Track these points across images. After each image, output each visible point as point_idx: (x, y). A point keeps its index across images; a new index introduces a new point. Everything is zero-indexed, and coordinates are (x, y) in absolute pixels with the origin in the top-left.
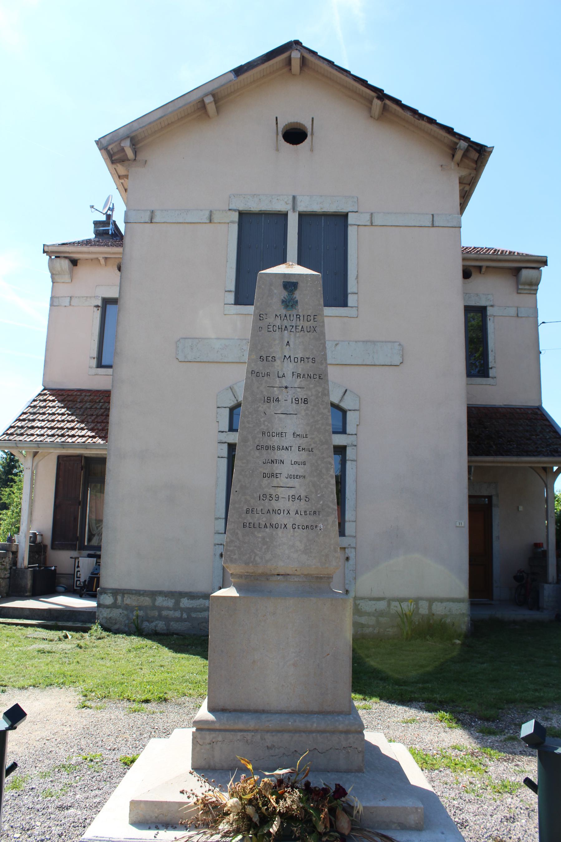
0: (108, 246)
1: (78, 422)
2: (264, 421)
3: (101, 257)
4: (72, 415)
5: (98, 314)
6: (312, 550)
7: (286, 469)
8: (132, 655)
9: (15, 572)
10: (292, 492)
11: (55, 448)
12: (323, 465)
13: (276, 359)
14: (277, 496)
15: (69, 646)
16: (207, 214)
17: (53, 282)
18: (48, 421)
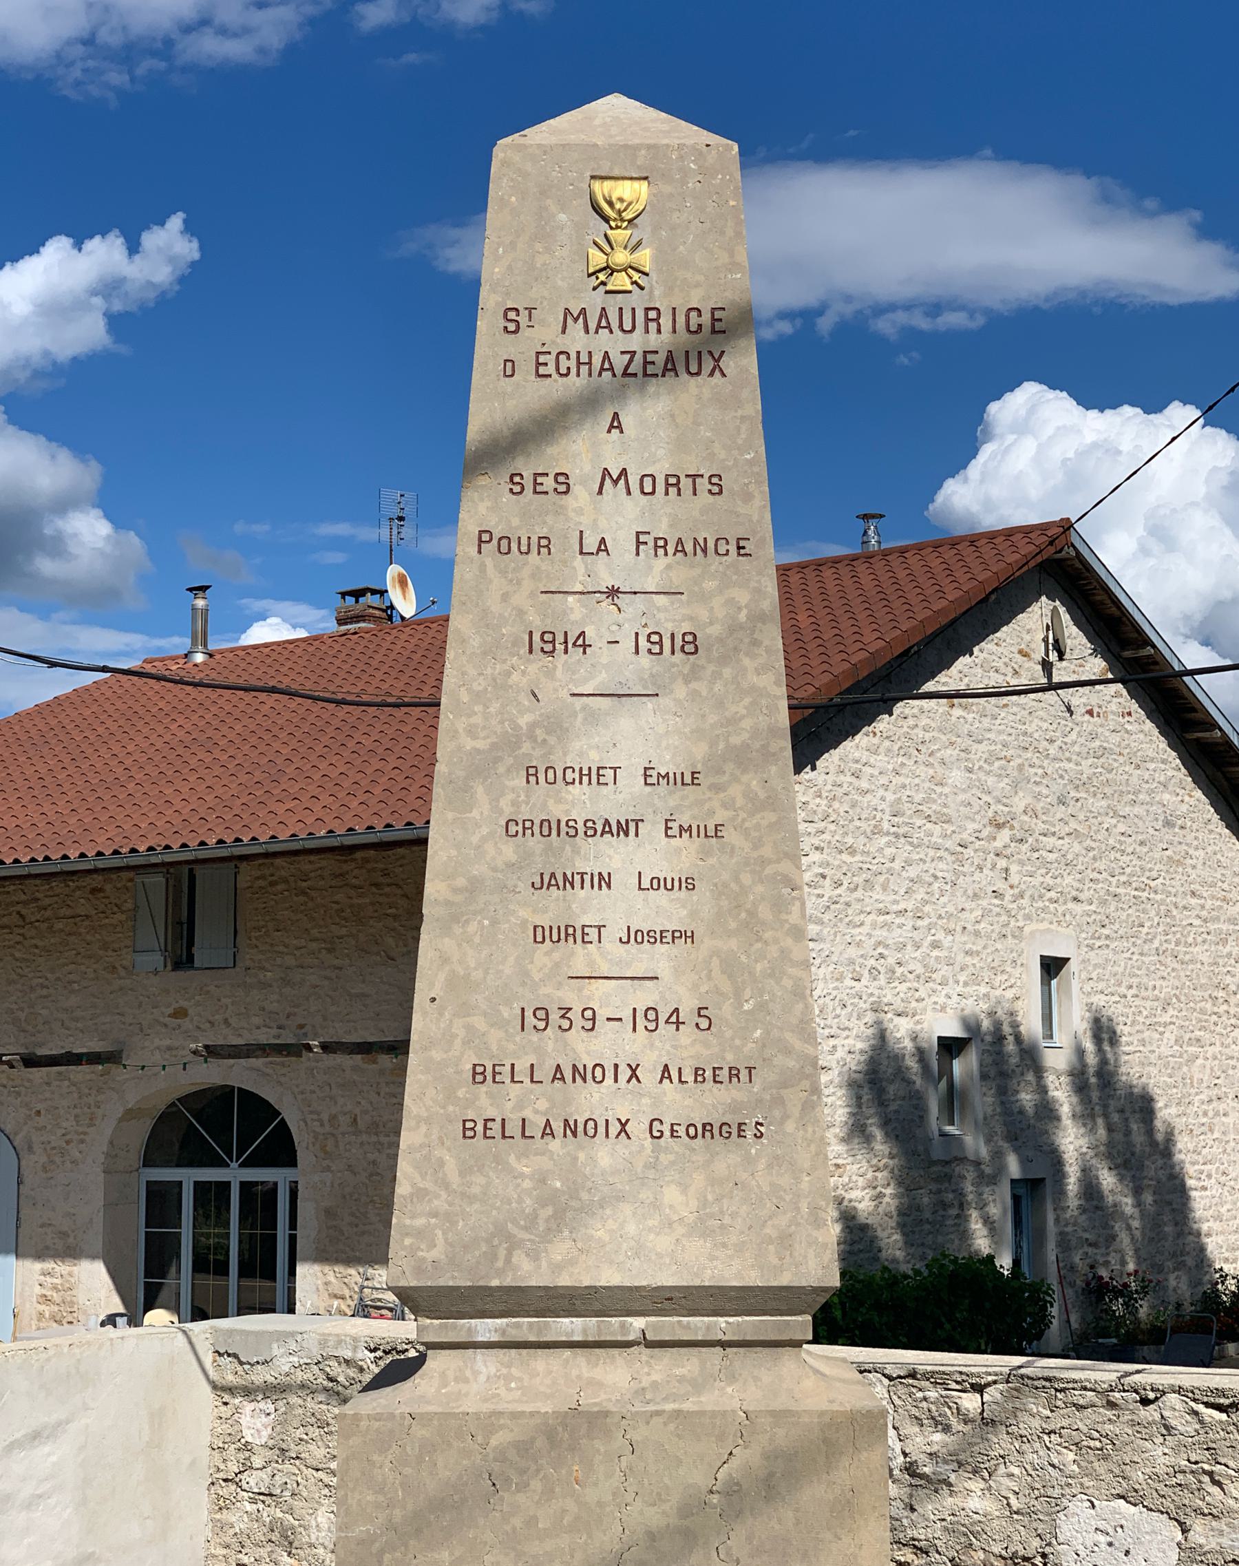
2: (533, 726)
6: (727, 1220)
7: (617, 909)
10: (644, 996)
12: (760, 889)
13: (571, 482)
14: (588, 1014)
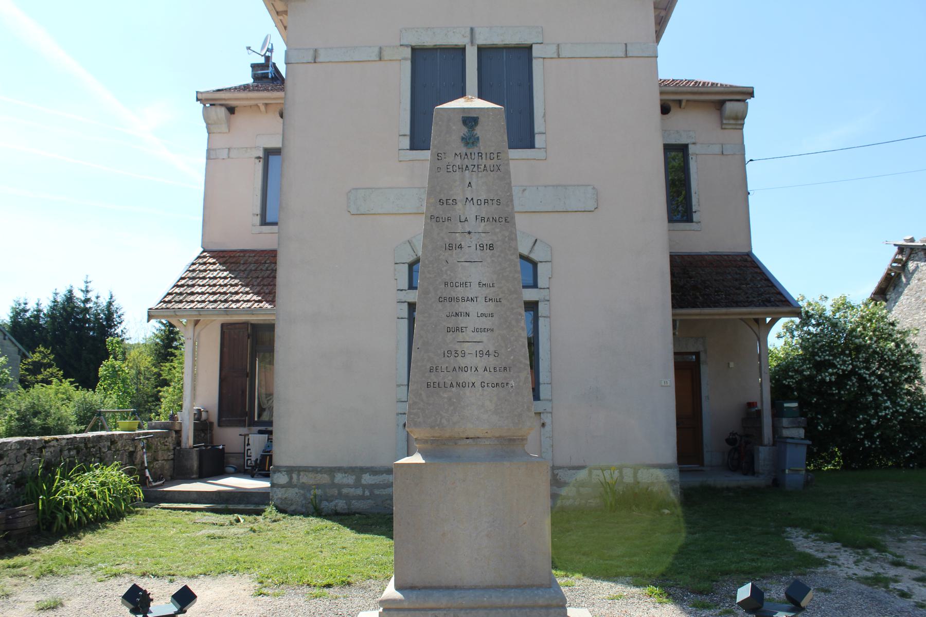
0: (268, 90)
1: (243, 286)
3: (260, 103)
4: (235, 278)
5: (260, 166)
7: (470, 323)
8: (310, 537)
9: (179, 452)
10: (479, 347)
11: (218, 315)
15: (242, 531)
16: (377, 50)
17: (209, 133)
18: (210, 286)
